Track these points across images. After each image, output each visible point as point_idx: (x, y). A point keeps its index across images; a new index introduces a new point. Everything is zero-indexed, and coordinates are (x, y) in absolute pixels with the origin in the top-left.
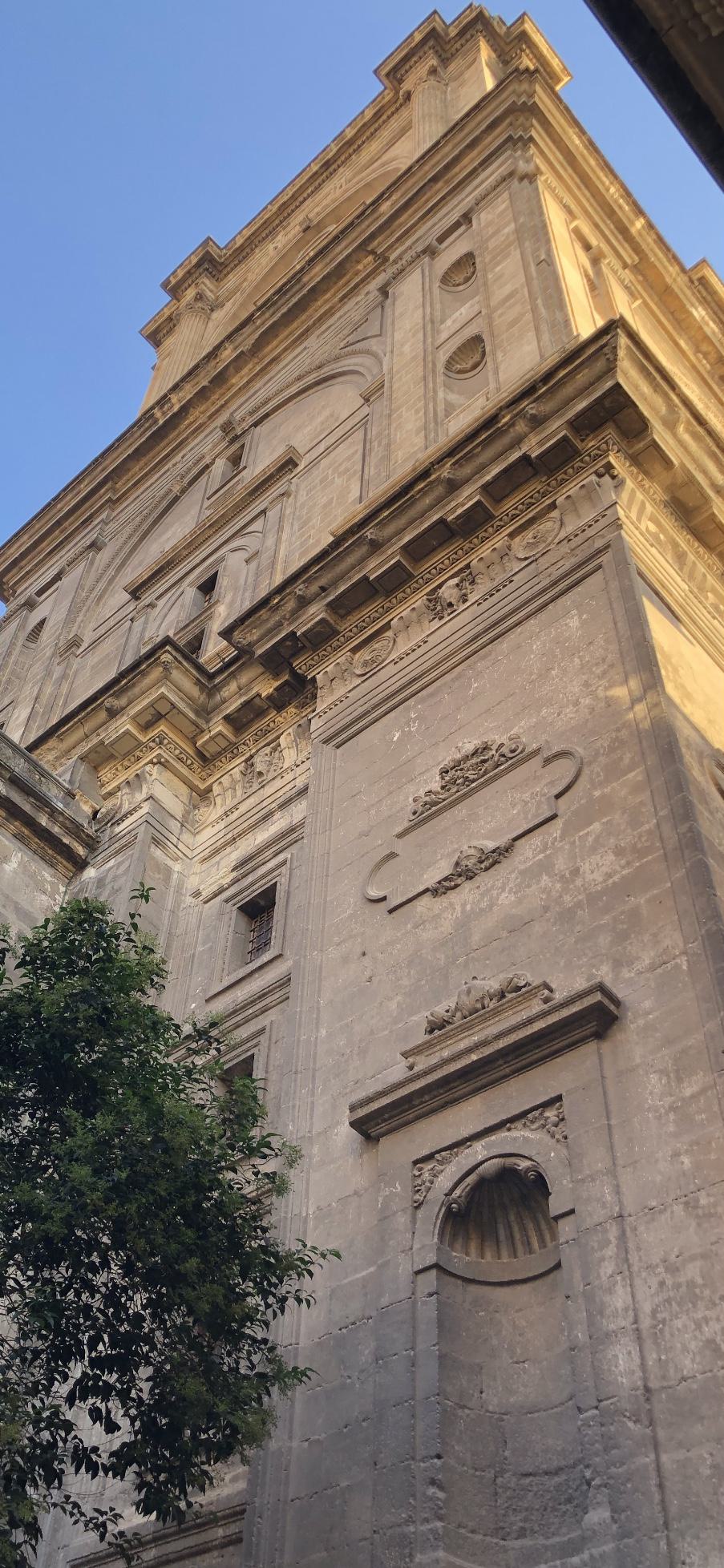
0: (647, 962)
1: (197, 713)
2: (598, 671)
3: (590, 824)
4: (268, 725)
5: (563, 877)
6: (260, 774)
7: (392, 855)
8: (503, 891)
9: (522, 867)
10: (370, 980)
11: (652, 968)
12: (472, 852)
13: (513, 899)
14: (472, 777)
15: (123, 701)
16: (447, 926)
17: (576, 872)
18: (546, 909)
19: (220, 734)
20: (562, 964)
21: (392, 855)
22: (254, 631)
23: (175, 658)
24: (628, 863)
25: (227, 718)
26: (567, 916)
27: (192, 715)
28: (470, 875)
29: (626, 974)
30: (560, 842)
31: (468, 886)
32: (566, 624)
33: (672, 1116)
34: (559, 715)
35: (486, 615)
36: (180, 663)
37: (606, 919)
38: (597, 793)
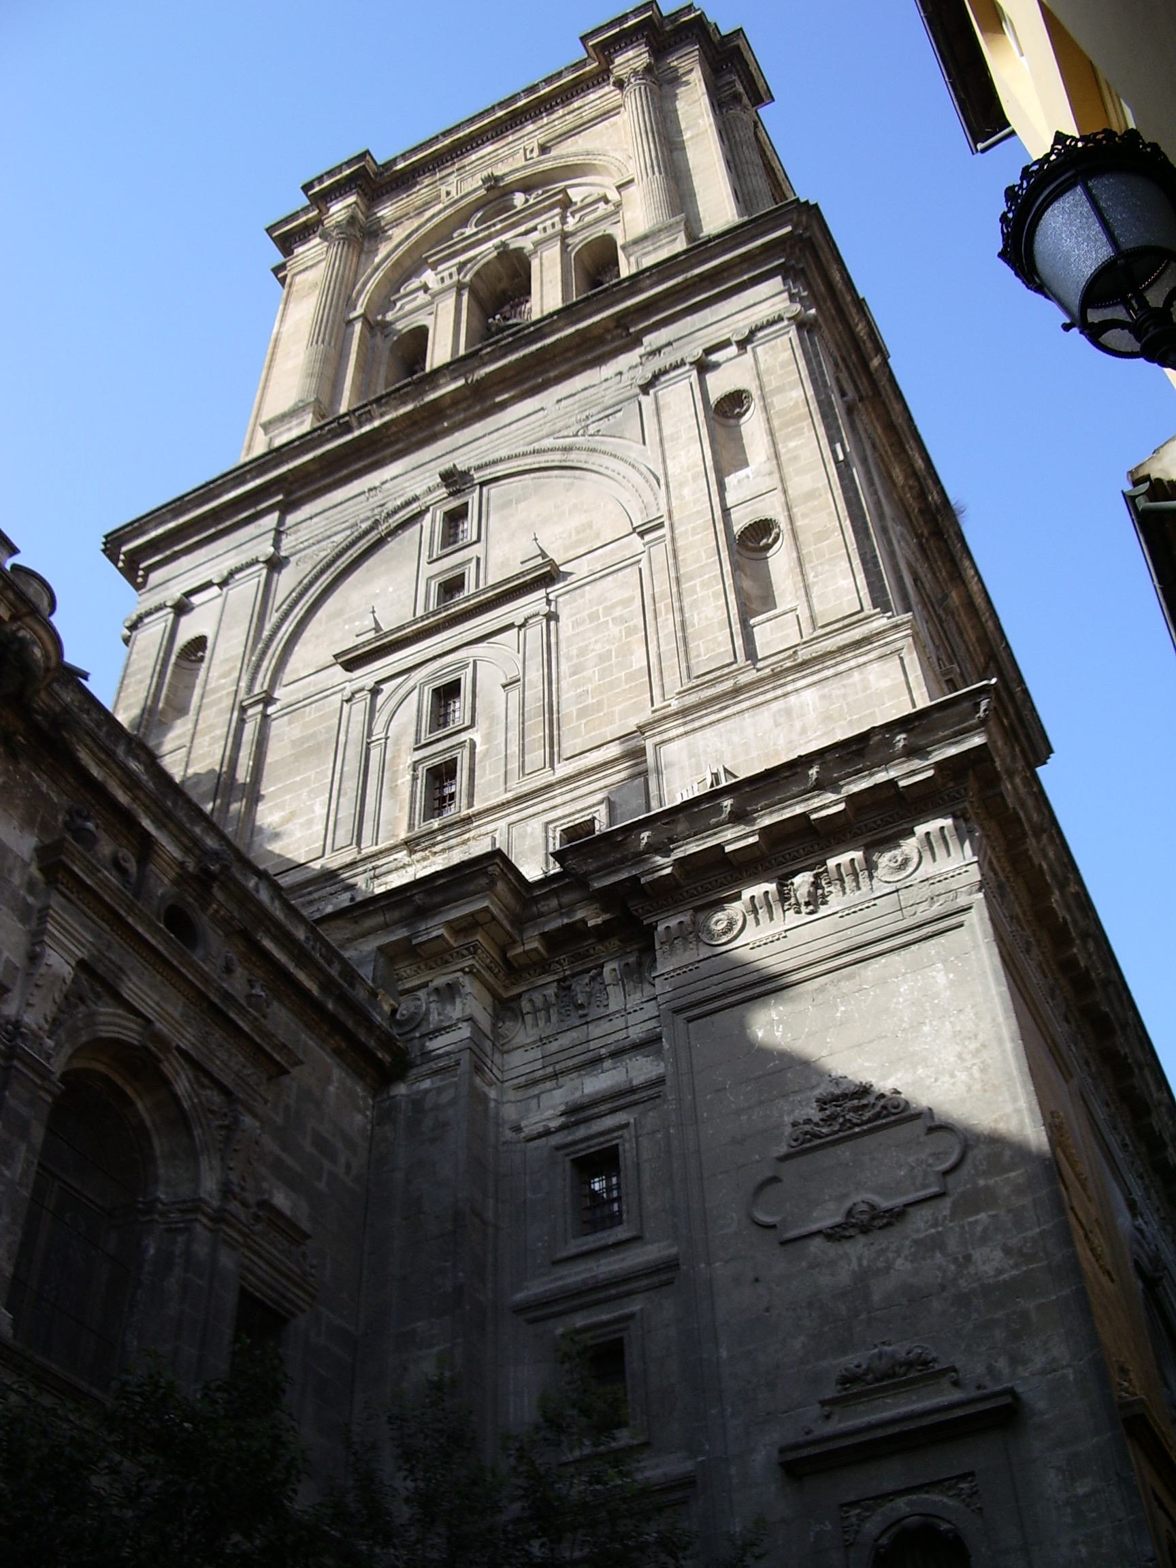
0: (1039, 1365)
1: (512, 924)
2: (973, 1046)
3: (977, 1213)
4: (587, 951)
5: (956, 1259)
6: (581, 1006)
7: (775, 1179)
8: (899, 1256)
9: (916, 1236)
10: (767, 1310)
11: (1043, 1372)
12: (865, 1207)
13: (909, 1267)
14: (855, 1121)
15: (438, 899)
16: (844, 1276)
17: (968, 1258)
18: (943, 1288)
19: (535, 949)
20: (963, 1346)
21: (775, 1179)
22: (590, 860)
23: (502, 870)
24: (1016, 1266)
25: (544, 936)
26: (963, 1300)
27: (509, 928)
28: (865, 1229)
29: (1021, 1371)
30: (951, 1221)
31: (862, 1239)
32: (933, 977)
33: (1069, 1510)
34: (936, 1080)
35: (848, 932)
36: (506, 875)
37: (999, 1314)
38: (981, 1182)
